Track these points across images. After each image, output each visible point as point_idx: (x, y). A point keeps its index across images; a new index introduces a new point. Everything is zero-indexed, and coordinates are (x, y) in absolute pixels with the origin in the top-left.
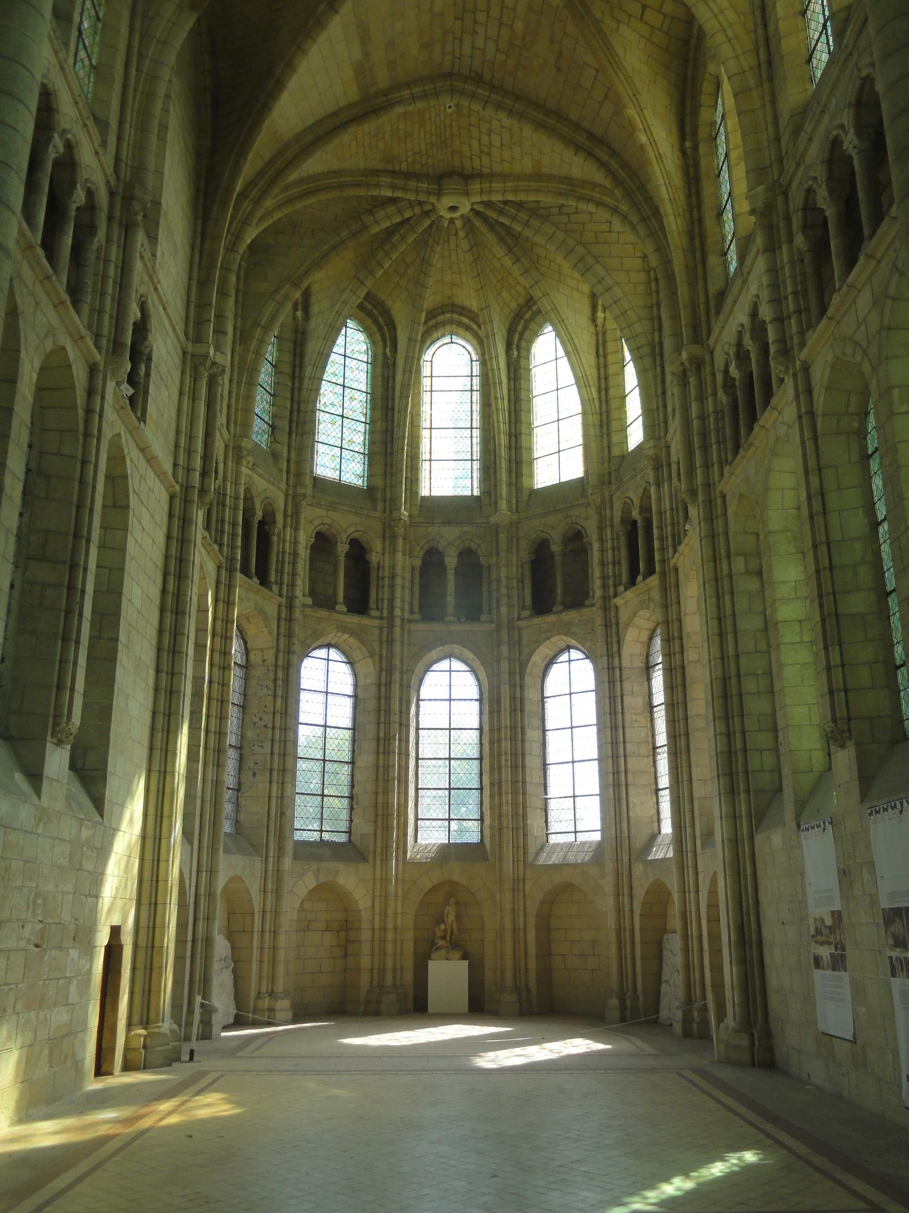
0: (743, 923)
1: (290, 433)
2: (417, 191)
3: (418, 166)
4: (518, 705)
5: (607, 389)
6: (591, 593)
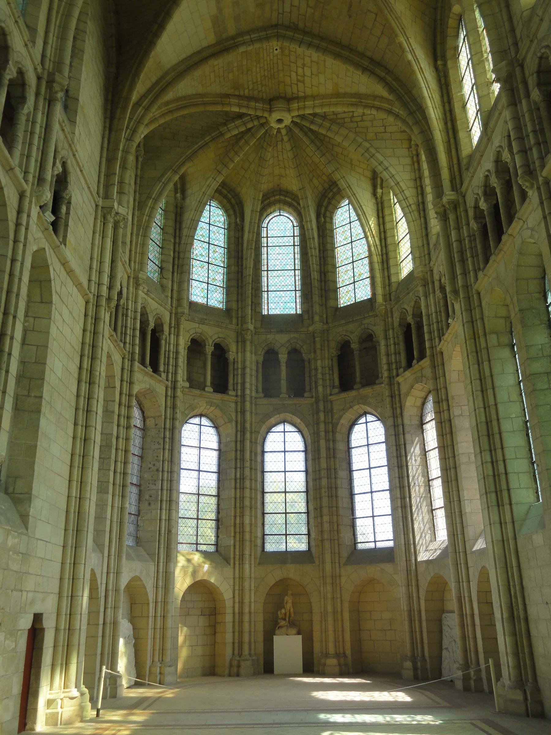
0: (512, 604)
1: (173, 273)
2: (256, 109)
3: (256, 92)
4: (332, 453)
5: (385, 239)
6: (380, 375)
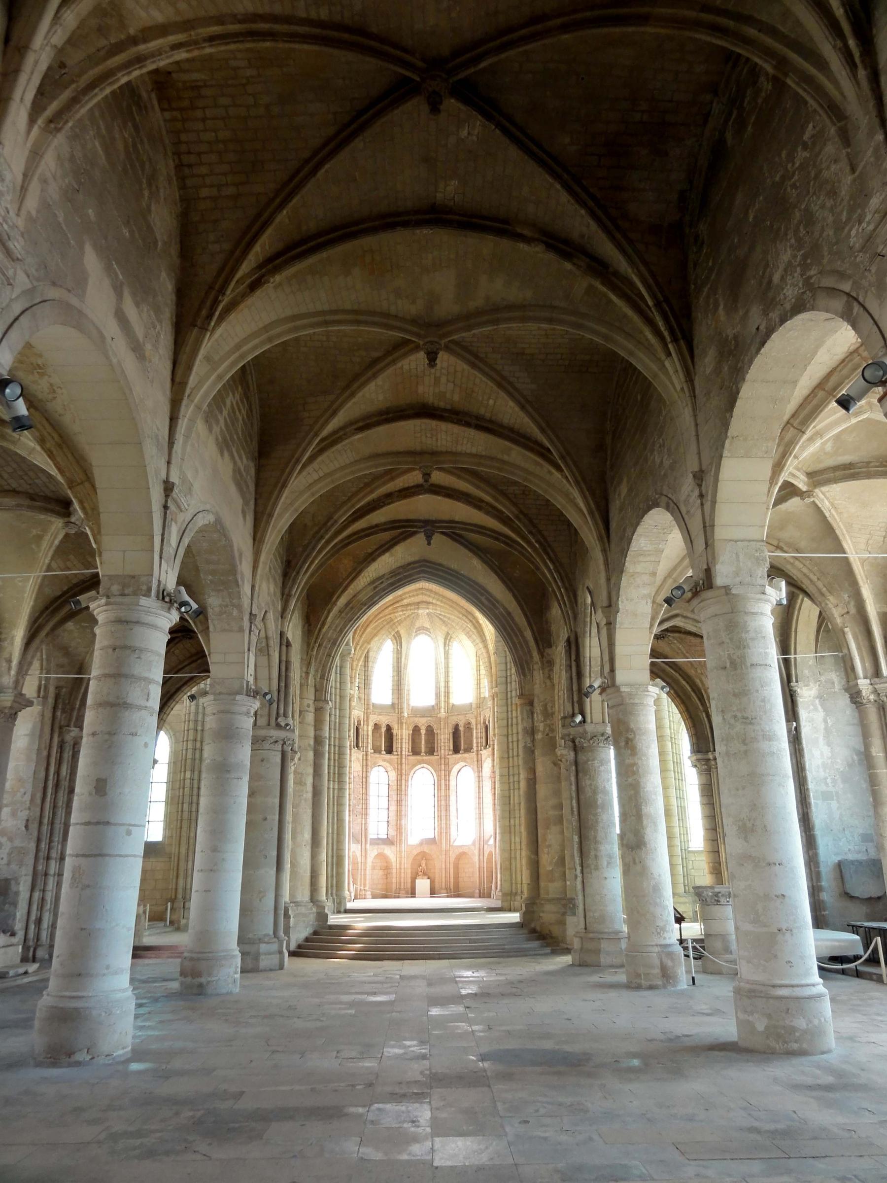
4: (447, 787)
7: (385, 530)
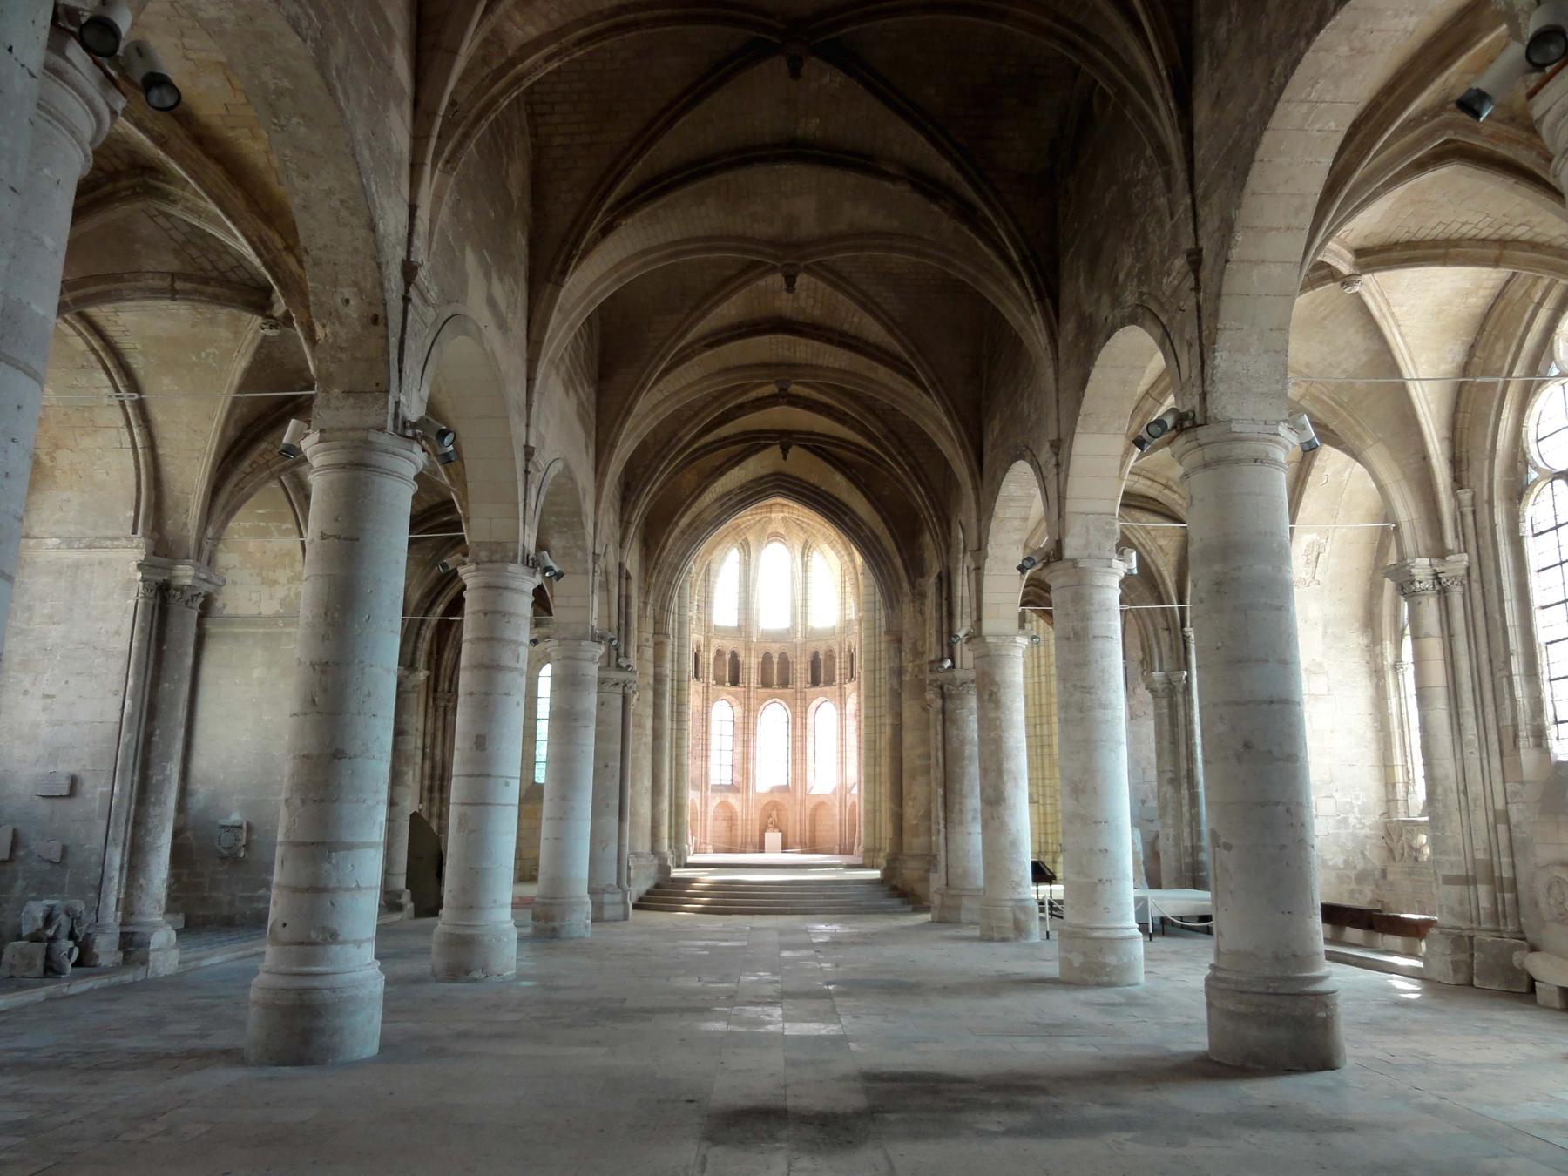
4: (804, 726)
7: (735, 443)
